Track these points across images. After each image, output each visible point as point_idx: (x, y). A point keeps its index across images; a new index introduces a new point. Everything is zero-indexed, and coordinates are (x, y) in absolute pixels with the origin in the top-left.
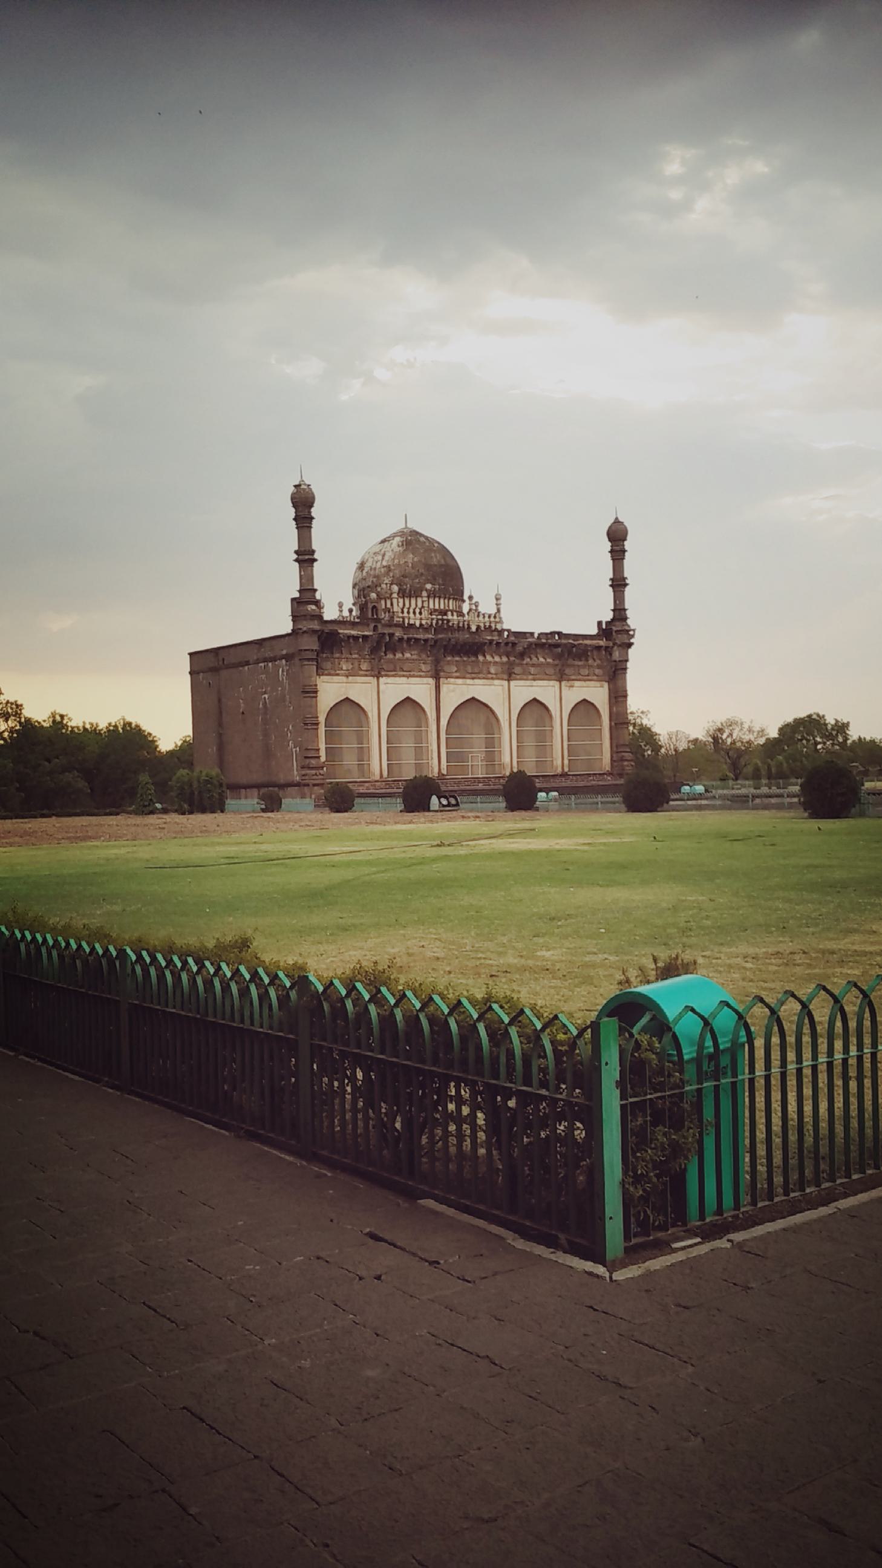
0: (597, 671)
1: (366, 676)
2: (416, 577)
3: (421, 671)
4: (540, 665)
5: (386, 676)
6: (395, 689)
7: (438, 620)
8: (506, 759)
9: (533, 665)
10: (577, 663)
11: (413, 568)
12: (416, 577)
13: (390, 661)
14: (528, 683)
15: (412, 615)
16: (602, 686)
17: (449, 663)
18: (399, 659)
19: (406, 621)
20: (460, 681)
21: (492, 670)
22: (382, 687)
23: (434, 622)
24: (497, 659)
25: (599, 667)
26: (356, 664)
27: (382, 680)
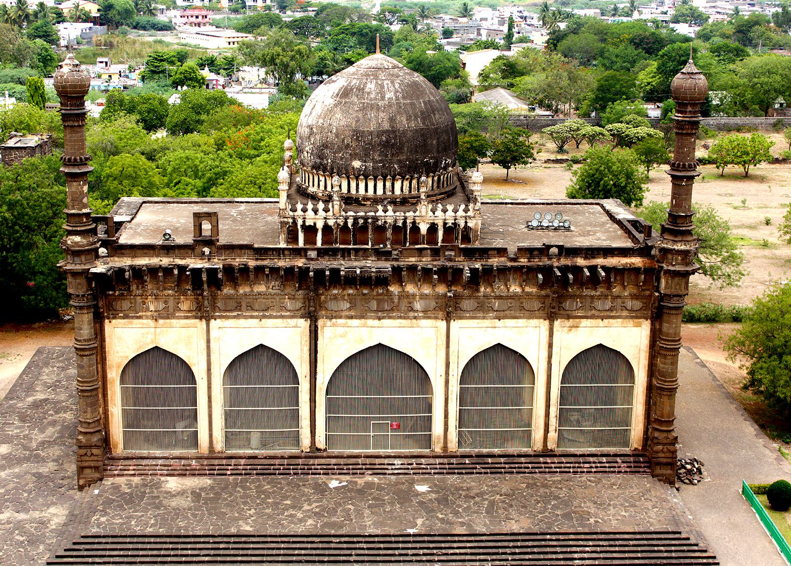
0: (629, 304)
1: (187, 318)
2: (340, 149)
5: (221, 317)
6: (235, 335)
7: (356, 219)
8: (437, 429)
9: (500, 297)
10: (587, 292)
11: (337, 136)
12: (340, 149)
13: (229, 297)
14: (487, 323)
15: (310, 213)
17: (335, 298)
19: (300, 222)
21: (418, 306)
23: (350, 222)
24: (427, 290)
25: (633, 297)
26: (171, 303)
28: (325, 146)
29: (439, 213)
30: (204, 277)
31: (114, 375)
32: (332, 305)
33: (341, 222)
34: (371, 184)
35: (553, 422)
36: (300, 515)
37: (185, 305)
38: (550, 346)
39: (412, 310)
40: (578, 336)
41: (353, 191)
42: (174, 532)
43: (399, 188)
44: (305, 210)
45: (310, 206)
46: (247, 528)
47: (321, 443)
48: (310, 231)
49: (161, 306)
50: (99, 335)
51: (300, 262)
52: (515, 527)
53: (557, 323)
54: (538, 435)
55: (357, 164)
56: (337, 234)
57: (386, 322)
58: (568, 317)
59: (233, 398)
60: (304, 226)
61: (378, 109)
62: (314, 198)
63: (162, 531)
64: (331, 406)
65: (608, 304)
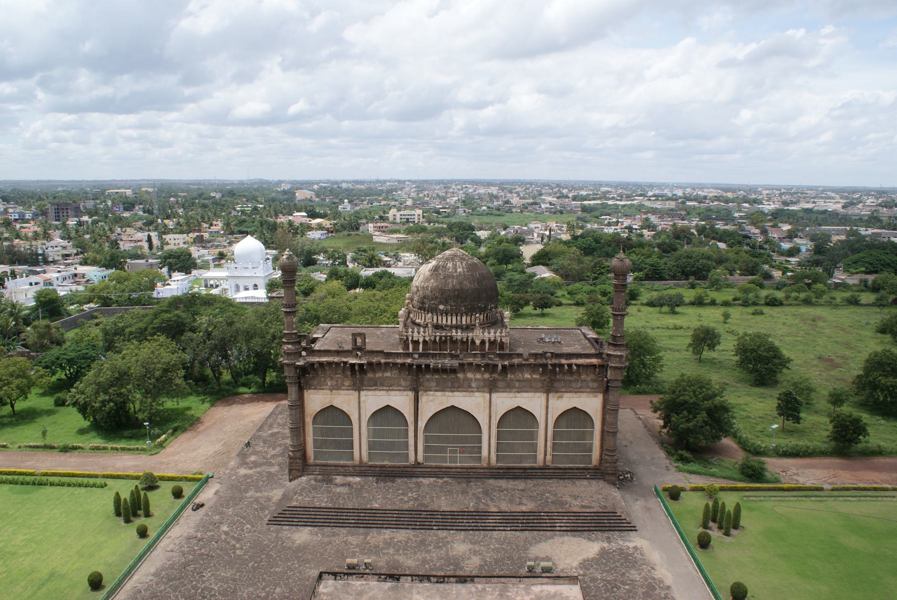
0: (591, 384)
3: (400, 385)
4: (527, 380)
6: (374, 400)
7: (441, 337)
8: (485, 453)
9: (518, 381)
11: (431, 292)
13: (371, 379)
14: (511, 395)
15: (416, 334)
16: (596, 397)
17: (428, 380)
18: (379, 378)
19: (410, 339)
20: (439, 393)
21: (473, 385)
22: (362, 398)
23: (438, 339)
24: (478, 376)
25: (593, 381)
26: (340, 382)
27: (362, 393)
28: (424, 297)
29: (486, 334)
30: (357, 368)
31: (309, 420)
32: (426, 384)
33: (433, 338)
34: (449, 318)
35: (549, 449)
36: (406, 499)
37: (347, 383)
38: (547, 407)
39: (470, 387)
40: (563, 403)
41: (440, 322)
42: (337, 506)
43: (465, 320)
44: (413, 332)
45: (416, 330)
46: (376, 506)
47: (420, 458)
48: (416, 343)
49: (334, 383)
50: (301, 398)
51: (409, 361)
52: (524, 508)
53: (551, 395)
54: (540, 457)
55: (441, 307)
56: (430, 345)
57: (456, 394)
58: (557, 392)
59: (374, 434)
60: (412, 341)
61: (453, 277)
62: (419, 325)
63: (330, 505)
64: (427, 439)
65: (579, 385)
